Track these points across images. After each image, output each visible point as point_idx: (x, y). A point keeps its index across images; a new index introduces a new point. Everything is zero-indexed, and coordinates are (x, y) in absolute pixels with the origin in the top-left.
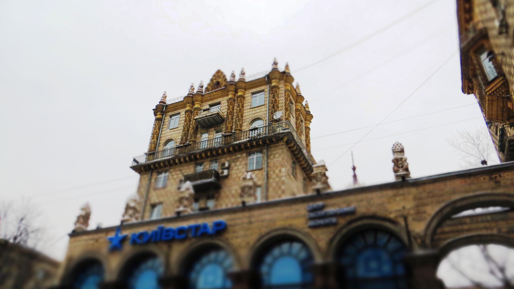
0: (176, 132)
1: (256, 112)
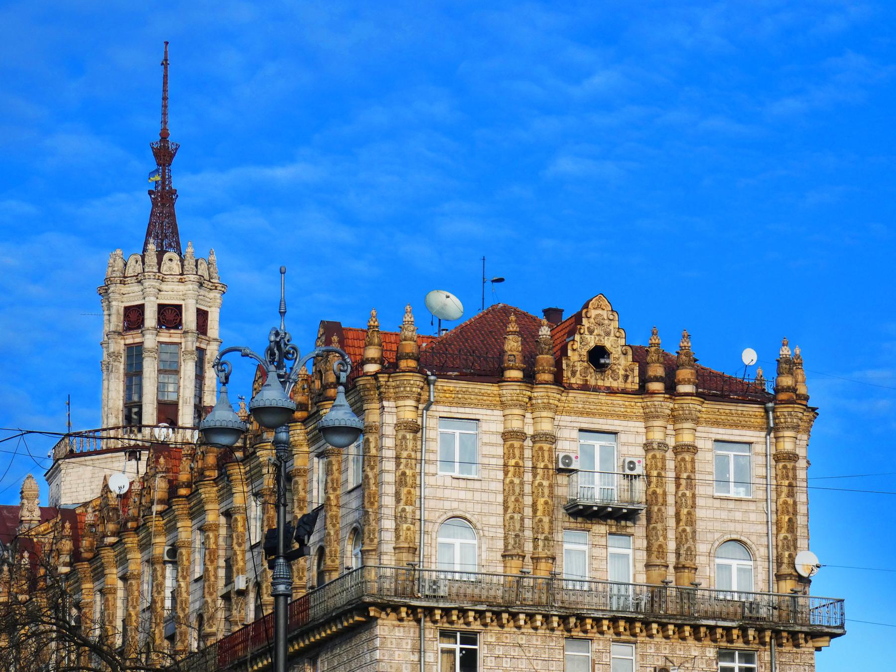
0: (477, 496)
1: (732, 515)
